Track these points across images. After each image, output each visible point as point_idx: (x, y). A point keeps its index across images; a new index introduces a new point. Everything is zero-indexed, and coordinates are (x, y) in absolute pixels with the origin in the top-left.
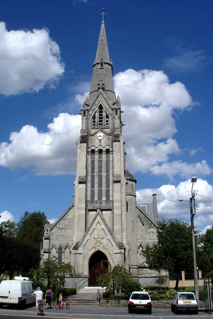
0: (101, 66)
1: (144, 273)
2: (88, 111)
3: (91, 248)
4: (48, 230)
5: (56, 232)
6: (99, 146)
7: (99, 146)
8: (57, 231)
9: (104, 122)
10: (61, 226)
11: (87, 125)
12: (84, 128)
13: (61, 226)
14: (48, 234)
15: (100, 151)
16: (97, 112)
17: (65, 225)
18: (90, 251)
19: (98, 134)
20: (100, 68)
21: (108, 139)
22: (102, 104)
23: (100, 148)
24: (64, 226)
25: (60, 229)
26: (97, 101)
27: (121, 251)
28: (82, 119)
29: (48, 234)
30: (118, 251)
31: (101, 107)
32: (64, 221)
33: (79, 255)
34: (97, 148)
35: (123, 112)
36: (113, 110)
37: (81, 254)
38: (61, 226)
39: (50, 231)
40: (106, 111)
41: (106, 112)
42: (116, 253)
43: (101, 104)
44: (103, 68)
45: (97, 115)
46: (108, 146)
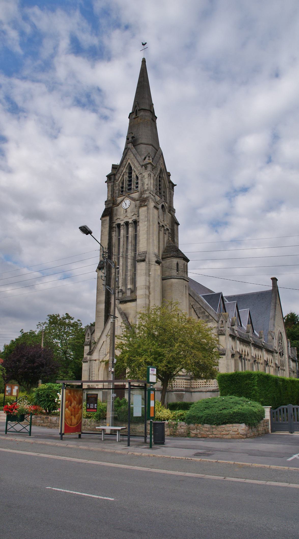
0: (135, 115)
1: (199, 386)
3: (107, 352)
6: (124, 218)
7: (124, 218)
12: (110, 198)
14: (89, 339)
15: (127, 224)
16: (125, 174)
18: (106, 357)
19: (123, 204)
21: (134, 207)
23: (126, 220)
26: (125, 161)
28: (108, 186)
29: (89, 339)
33: (94, 362)
34: (123, 220)
36: (142, 166)
37: (95, 360)
39: (92, 334)
43: (129, 163)
44: (138, 117)
45: (126, 177)
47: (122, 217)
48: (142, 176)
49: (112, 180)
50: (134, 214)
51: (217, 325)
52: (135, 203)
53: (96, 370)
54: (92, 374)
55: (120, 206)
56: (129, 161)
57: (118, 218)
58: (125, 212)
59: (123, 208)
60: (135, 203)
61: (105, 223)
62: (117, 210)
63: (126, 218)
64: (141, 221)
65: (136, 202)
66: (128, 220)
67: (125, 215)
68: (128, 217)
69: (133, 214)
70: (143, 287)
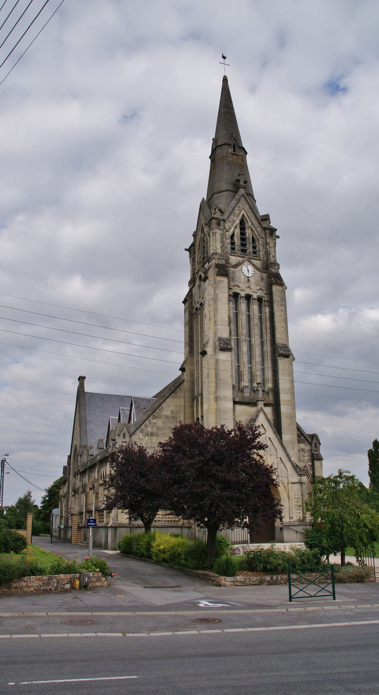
0: (233, 150)
2: (224, 221)
4: (124, 434)
5: (142, 440)
6: (246, 288)
7: (246, 288)
8: (142, 437)
9: (250, 249)
10: (149, 429)
11: (223, 246)
13: (150, 428)
15: (248, 297)
17: (157, 428)
20: (232, 154)
21: (260, 279)
22: (245, 215)
23: (248, 292)
24: (155, 430)
25: (147, 434)
26: (236, 208)
27: (300, 479)
30: (296, 479)
31: (242, 222)
32: (155, 421)
34: (244, 291)
38: (150, 428)
40: (254, 229)
41: (252, 230)
42: (293, 483)
45: (238, 231)
46: (260, 291)
47: (242, 286)
48: (264, 242)
49: (222, 227)
50: (261, 289)
51: (310, 448)
52: (261, 274)
55: (238, 268)
56: (243, 212)
57: (236, 285)
58: (246, 280)
59: (244, 274)
60: (261, 274)
61: (222, 286)
62: (234, 272)
63: (248, 288)
64: (276, 303)
65: (262, 273)
66: (239, 292)
67: (248, 285)
68: (251, 289)
69: (259, 288)
70: (287, 390)
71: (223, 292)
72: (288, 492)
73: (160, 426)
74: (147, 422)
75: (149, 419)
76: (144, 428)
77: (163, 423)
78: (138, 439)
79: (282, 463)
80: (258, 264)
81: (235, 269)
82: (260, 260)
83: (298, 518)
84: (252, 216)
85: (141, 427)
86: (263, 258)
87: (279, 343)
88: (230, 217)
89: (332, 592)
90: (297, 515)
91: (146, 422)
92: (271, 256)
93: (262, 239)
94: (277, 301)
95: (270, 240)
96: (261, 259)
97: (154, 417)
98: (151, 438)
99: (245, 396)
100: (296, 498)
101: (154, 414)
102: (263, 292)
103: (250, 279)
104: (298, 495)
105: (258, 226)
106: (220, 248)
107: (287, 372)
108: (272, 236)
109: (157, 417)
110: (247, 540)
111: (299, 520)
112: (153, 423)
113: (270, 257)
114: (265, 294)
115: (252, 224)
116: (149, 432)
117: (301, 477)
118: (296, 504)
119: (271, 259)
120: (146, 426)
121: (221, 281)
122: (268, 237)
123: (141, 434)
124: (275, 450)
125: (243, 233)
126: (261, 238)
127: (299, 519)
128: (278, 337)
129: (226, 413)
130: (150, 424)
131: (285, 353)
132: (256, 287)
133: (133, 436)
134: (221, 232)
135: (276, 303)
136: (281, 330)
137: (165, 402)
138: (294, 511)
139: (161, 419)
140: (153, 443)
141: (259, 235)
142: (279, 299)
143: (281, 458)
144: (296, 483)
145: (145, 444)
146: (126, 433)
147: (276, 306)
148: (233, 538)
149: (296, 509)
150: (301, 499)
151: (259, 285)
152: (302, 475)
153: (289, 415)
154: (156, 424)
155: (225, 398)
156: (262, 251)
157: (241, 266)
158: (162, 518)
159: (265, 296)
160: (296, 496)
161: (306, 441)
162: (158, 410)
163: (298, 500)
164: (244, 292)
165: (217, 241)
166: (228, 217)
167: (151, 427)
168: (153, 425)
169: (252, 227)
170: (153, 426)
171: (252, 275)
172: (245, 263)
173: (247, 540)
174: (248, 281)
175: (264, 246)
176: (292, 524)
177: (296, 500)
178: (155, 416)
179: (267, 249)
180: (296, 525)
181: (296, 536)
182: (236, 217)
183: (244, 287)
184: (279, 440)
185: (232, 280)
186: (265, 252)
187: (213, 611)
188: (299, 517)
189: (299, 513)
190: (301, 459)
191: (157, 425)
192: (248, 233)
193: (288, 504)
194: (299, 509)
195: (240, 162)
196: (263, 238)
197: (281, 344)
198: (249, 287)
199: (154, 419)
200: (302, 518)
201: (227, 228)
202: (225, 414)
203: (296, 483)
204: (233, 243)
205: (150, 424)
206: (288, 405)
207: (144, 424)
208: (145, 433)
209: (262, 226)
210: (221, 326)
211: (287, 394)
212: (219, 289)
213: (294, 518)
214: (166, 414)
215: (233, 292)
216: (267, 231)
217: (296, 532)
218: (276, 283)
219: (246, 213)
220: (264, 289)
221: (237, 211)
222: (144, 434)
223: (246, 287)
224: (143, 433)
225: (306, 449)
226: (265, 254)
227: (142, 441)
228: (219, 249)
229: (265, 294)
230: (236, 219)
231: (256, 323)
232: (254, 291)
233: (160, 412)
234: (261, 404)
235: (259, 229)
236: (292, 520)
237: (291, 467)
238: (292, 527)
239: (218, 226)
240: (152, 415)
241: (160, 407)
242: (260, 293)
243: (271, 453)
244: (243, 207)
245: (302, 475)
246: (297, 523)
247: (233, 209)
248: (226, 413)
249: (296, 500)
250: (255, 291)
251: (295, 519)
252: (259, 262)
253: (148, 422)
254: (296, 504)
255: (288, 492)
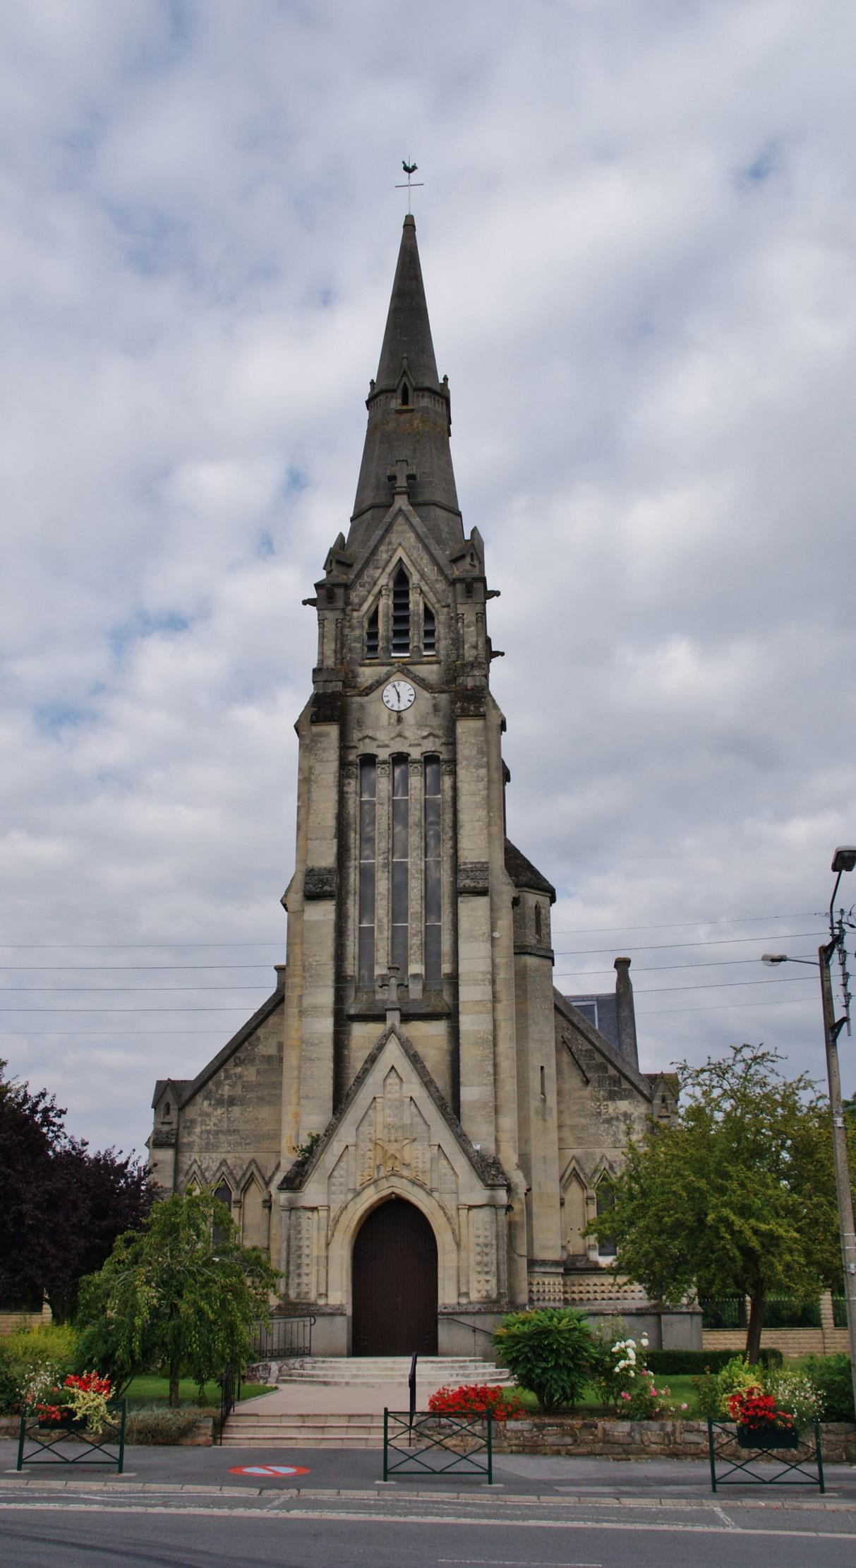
0: (400, 401)
1: (591, 1296)
2: (347, 587)
3: (358, 1183)
4: (168, 1105)
5: (209, 1115)
6: (393, 739)
7: (393, 739)
8: (209, 1110)
9: (416, 638)
10: (226, 1090)
11: (342, 648)
12: (330, 662)
13: (227, 1088)
14: (170, 1123)
15: (400, 759)
16: (384, 592)
17: (243, 1087)
18: (358, 1199)
19: (389, 692)
20: (399, 412)
21: (431, 709)
22: (405, 559)
23: (399, 746)
24: (238, 1091)
25: (220, 1102)
26: (383, 548)
27: (492, 1197)
28: (321, 622)
29: (170, 1123)
30: (480, 1195)
31: (401, 579)
32: (239, 1070)
33: (309, 1214)
34: (387, 746)
35: (497, 594)
36: (453, 583)
37: (314, 1209)
38: (227, 1088)
39: (181, 1109)
40: (425, 588)
41: (422, 592)
42: (471, 1207)
43: (400, 559)
44: (412, 411)
45: (386, 603)
46: (431, 738)
47: (382, 736)
48: (452, 615)
49: (340, 604)
50: (431, 734)
51: (648, 1109)
52: (434, 698)
53: (315, 1241)
54: (300, 1256)
55: (374, 695)
56: (400, 553)
57: (368, 737)
58: (393, 720)
59: (389, 705)
60: (434, 698)
61: (324, 745)
62: (362, 707)
63: (398, 739)
64: (465, 763)
65: (436, 695)
67: (397, 731)
68: (405, 738)
69: (425, 733)
70: (480, 977)
71: (324, 759)
72: (459, 1228)
73: (251, 1082)
74: (222, 1074)
75: (225, 1067)
76: (214, 1088)
77: (258, 1072)
78: (200, 1115)
79: (443, 1157)
80: (432, 672)
81: (366, 698)
82: (438, 662)
83: (484, 1293)
84: (422, 558)
85: (206, 1087)
86: (448, 656)
87: (467, 861)
88: (365, 573)
89: (118, 1457)
90: (480, 1288)
91: (217, 1075)
92: (466, 647)
93: (445, 610)
94: (467, 758)
95: (467, 606)
96: (442, 658)
97: (238, 1061)
98: (230, 1109)
99: (378, 1001)
100: (478, 1245)
101: (238, 1054)
102: (437, 740)
103: (404, 715)
104: (486, 1237)
105: (437, 580)
106: (333, 656)
107: (481, 932)
108: (471, 597)
109: (245, 1059)
110: (308, 1345)
111: (486, 1300)
112: (235, 1074)
113: (464, 649)
114: (443, 744)
115: (423, 576)
116: (226, 1097)
117: (493, 1192)
118: (479, 1258)
119: (467, 654)
120: (219, 1084)
121: (321, 735)
122: (459, 600)
123: (206, 1103)
124: (425, 1127)
125: (401, 604)
126: (444, 607)
127: (488, 1297)
128: (465, 846)
129: (317, 1044)
130: (227, 1077)
131: (473, 885)
132: (419, 732)
133: (187, 1108)
134: (338, 614)
135: (465, 763)
136: (474, 828)
137: (263, 1025)
138: (474, 1277)
139: (253, 1066)
140: (234, 1121)
141: (439, 601)
142: (474, 752)
143: (439, 1146)
144: (481, 1206)
145: (215, 1124)
146: (171, 1103)
147: (463, 771)
148: (301, 1339)
149: (479, 1272)
150: (495, 1247)
151: (427, 726)
152: (496, 1186)
153: (480, 1038)
154: (240, 1076)
155: (315, 1009)
156: (445, 639)
157: (382, 688)
158: (610, 1292)
159: (442, 749)
160: (481, 1240)
161: (635, 1092)
162: (246, 1043)
163: (487, 1250)
164: (386, 749)
165: (325, 640)
166: (360, 574)
167: (230, 1086)
168: (234, 1079)
169: (422, 584)
170: (235, 1083)
171: (410, 704)
172: (391, 679)
173: (308, 1345)
174: (399, 720)
175: (450, 626)
176: (463, 1309)
177: (479, 1249)
178: (239, 1058)
179: (458, 632)
180: (474, 1314)
181: (472, 1341)
182: (380, 571)
183: (388, 738)
184: (435, 1102)
185: (356, 727)
186: (452, 639)
187: (225, 1512)
188: (487, 1291)
189: (487, 1281)
190: (620, 1141)
191: (245, 1079)
192: (415, 602)
193: (456, 1260)
194: (487, 1273)
195: (418, 427)
196: (448, 606)
197: (472, 863)
198: (400, 735)
199: (236, 1065)
200: (494, 1296)
201: (356, 600)
202: (312, 1048)
203: (481, 1206)
204: (373, 635)
205: (227, 1077)
206: (481, 1013)
207: (214, 1079)
208: (216, 1100)
209: (446, 577)
210: (318, 842)
211: (479, 985)
212: (316, 754)
213: (471, 1295)
214: (264, 1053)
215: (360, 753)
216: (459, 587)
217: (474, 1331)
218: (465, 714)
219: (407, 554)
220: (440, 733)
221: (383, 556)
222: (213, 1102)
223: (393, 735)
224: (210, 1100)
225: (636, 1114)
226: (452, 644)
227: (207, 1119)
228: (330, 657)
229: (443, 744)
230: (377, 575)
231: (417, 819)
232: (412, 742)
233: (253, 1050)
234: (393, 1018)
235: (441, 586)
236: (464, 1301)
237: (467, 1168)
238: (462, 1319)
239: (329, 603)
240: (232, 1059)
241: (253, 1038)
242: (430, 746)
243: (415, 1135)
244: (398, 541)
245: (496, 1186)
246: (477, 1307)
247: (374, 551)
248: (317, 1044)
249: (479, 1249)
250: (416, 742)
251: (474, 1296)
252: (435, 667)
253: (223, 1074)
254: (479, 1258)
255: (459, 1228)
